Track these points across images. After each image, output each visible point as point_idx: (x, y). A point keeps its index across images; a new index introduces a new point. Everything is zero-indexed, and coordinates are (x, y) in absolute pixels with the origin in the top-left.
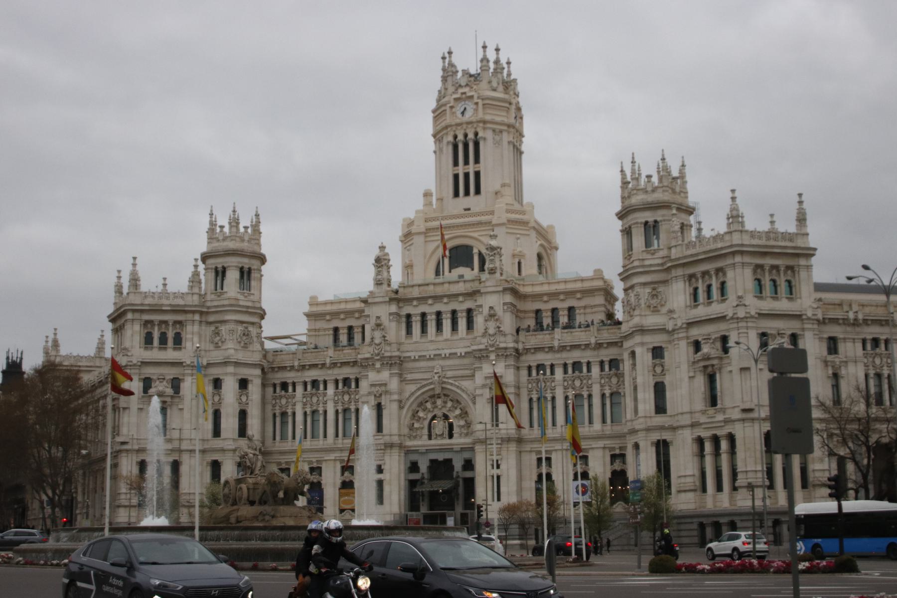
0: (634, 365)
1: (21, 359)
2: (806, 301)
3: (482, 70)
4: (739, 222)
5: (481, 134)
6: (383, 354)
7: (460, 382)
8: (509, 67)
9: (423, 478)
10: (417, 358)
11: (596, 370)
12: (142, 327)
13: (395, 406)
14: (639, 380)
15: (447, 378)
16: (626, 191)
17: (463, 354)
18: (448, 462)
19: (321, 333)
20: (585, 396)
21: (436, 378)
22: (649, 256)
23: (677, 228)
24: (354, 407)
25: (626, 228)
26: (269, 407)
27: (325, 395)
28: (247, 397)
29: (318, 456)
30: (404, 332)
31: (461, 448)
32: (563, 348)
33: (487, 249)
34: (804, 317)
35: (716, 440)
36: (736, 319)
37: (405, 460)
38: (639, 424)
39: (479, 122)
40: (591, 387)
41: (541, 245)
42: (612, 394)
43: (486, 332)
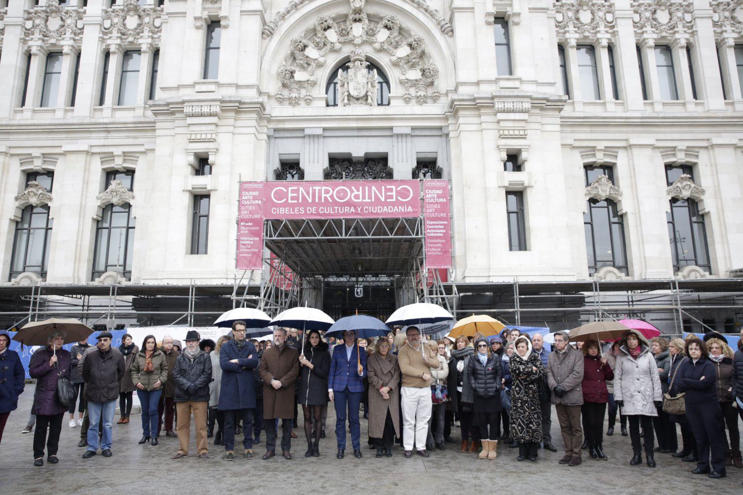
13: (253, 25)
24: (150, 41)
29: (49, 143)
31: (413, 128)
37: (268, 154)
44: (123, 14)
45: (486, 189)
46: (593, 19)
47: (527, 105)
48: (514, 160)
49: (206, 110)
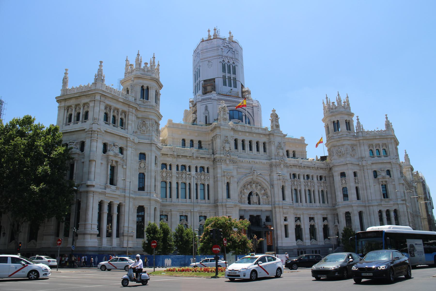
11: (315, 179)
13: (236, 185)
25: (334, 122)
35: (388, 212)
43: (278, 154)
44: (200, 175)
45: (281, 225)
47: (288, 208)
49: (231, 207)
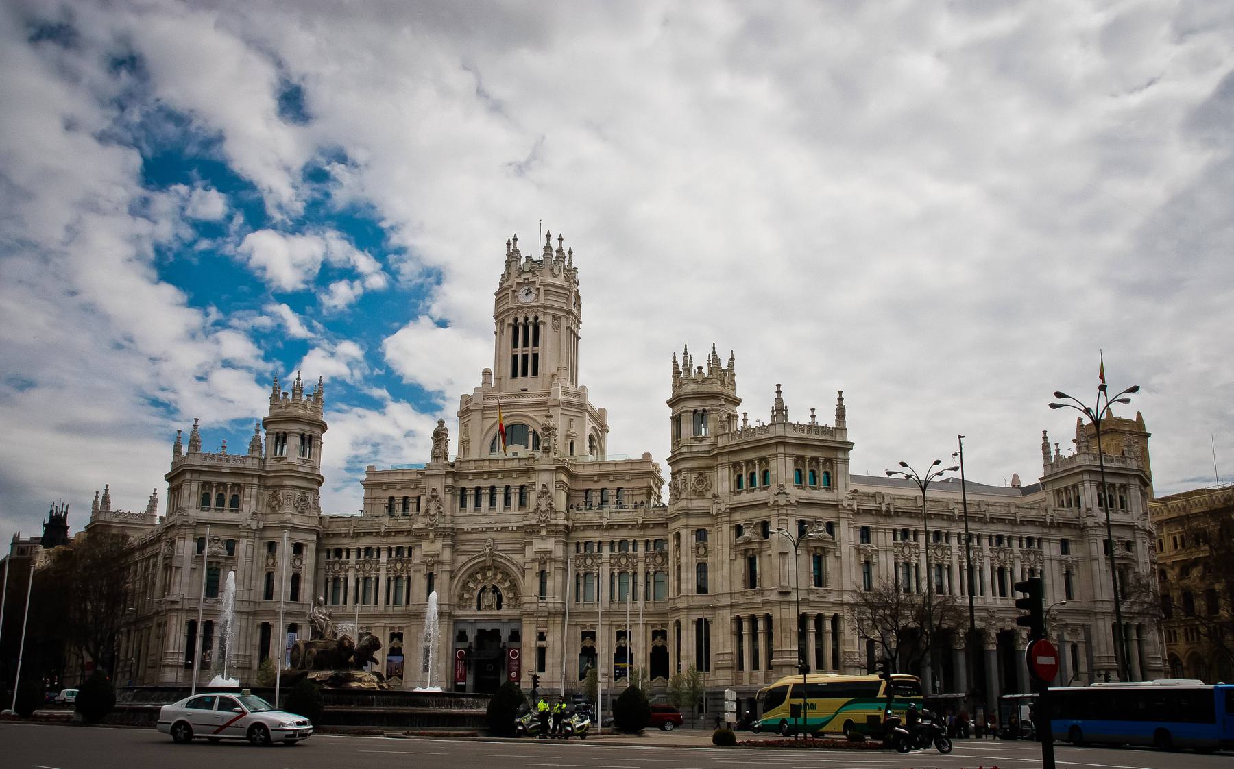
0: (678, 546)
1: (66, 513)
2: (842, 493)
3: (544, 258)
4: (783, 415)
5: (541, 318)
6: (437, 525)
7: (510, 555)
8: (570, 256)
9: (470, 647)
10: (470, 530)
11: (641, 549)
12: (200, 490)
13: (446, 577)
14: (683, 560)
15: (498, 551)
16: (678, 380)
17: (515, 529)
18: (495, 634)
19: (377, 502)
20: (630, 574)
21: (488, 550)
22: (696, 443)
23: (725, 417)
24: (406, 575)
26: (322, 573)
27: (378, 562)
28: (301, 561)
29: (369, 622)
30: (458, 505)
32: (610, 527)
33: (542, 429)
34: (840, 507)
35: (753, 620)
36: (776, 505)
38: (682, 603)
39: (539, 307)
40: (636, 565)
41: (593, 427)
42: (655, 573)
43: (538, 508)
45: (531, 648)
46: (592, 563)
47: (546, 615)
48: (542, 637)
